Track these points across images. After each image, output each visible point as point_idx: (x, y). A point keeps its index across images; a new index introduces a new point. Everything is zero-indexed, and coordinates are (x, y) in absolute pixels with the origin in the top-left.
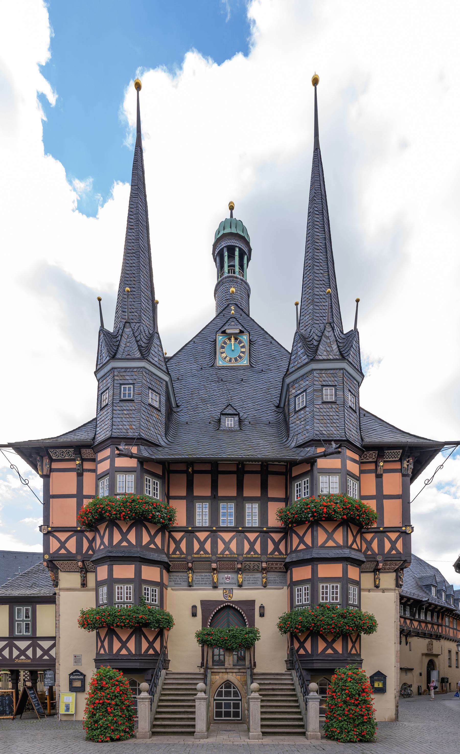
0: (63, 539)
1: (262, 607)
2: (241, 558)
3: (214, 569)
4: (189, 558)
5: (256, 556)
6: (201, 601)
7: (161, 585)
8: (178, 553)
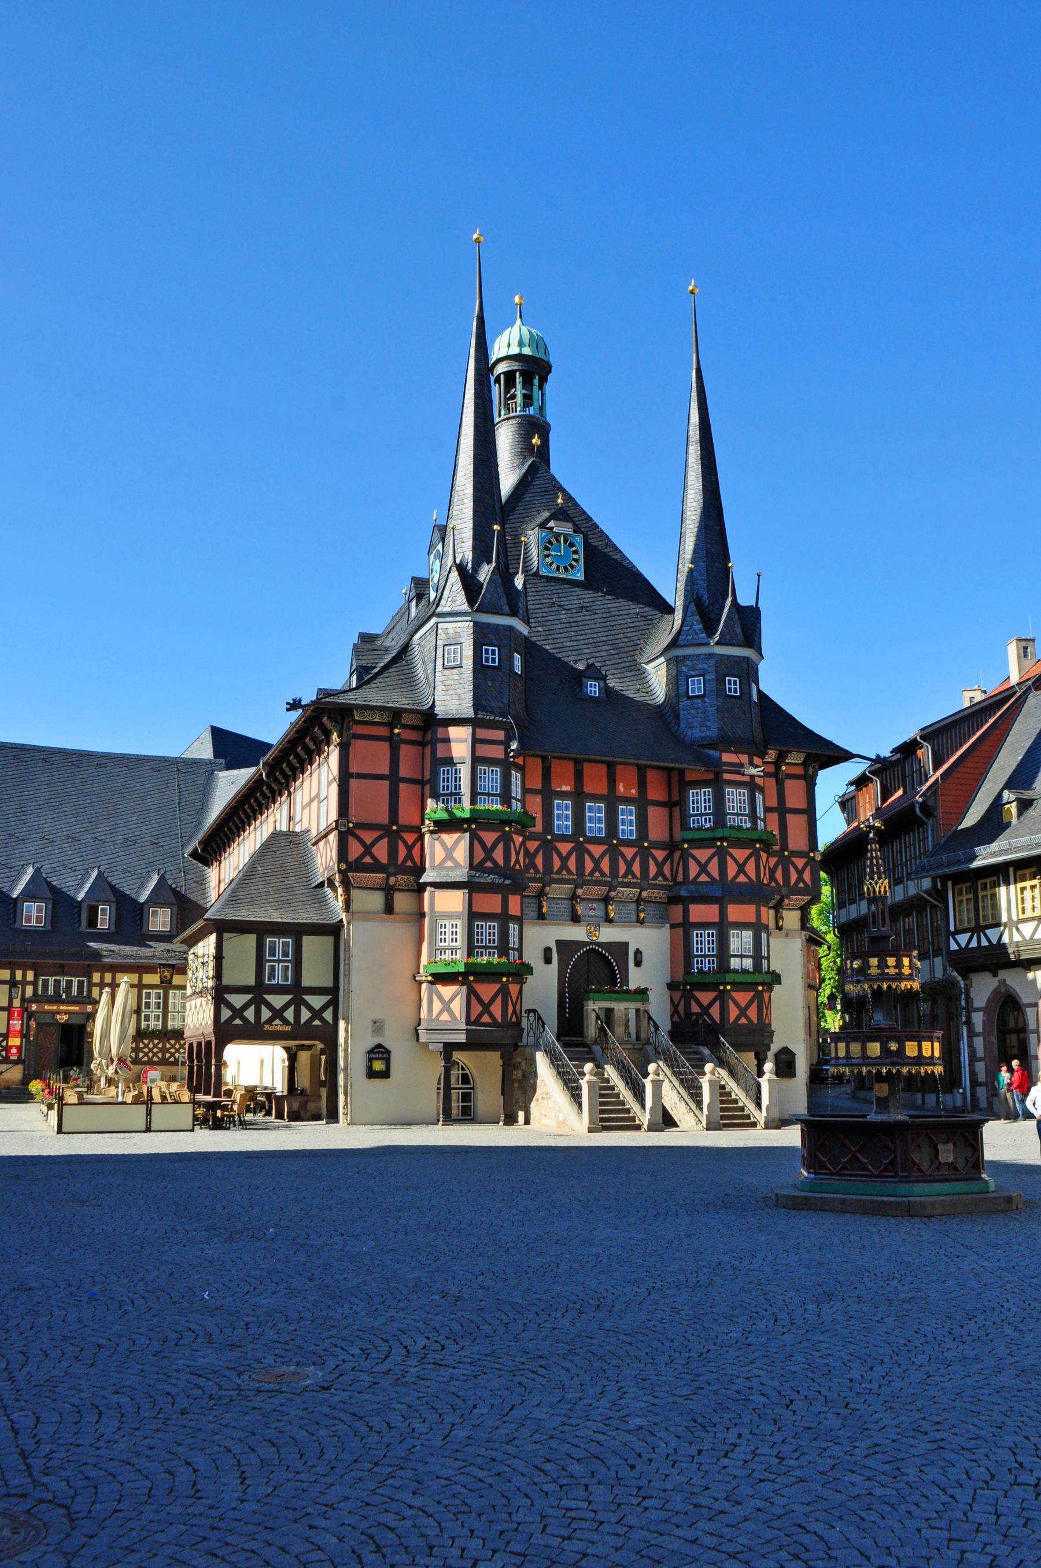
0: (368, 842)
1: (638, 952)
2: (615, 883)
3: (579, 897)
4: (547, 879)
5: (635, 880)
6: (557, 941)
7: (519, 920)
8: (532, 871)
